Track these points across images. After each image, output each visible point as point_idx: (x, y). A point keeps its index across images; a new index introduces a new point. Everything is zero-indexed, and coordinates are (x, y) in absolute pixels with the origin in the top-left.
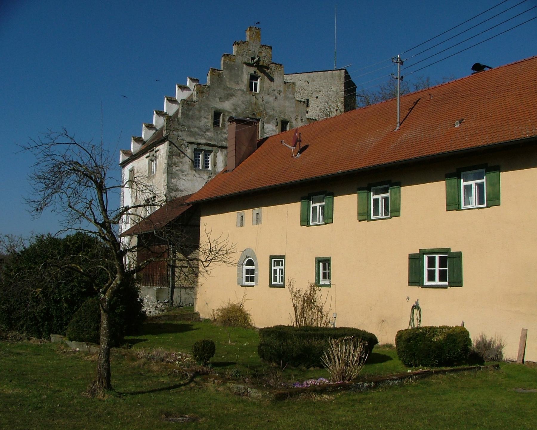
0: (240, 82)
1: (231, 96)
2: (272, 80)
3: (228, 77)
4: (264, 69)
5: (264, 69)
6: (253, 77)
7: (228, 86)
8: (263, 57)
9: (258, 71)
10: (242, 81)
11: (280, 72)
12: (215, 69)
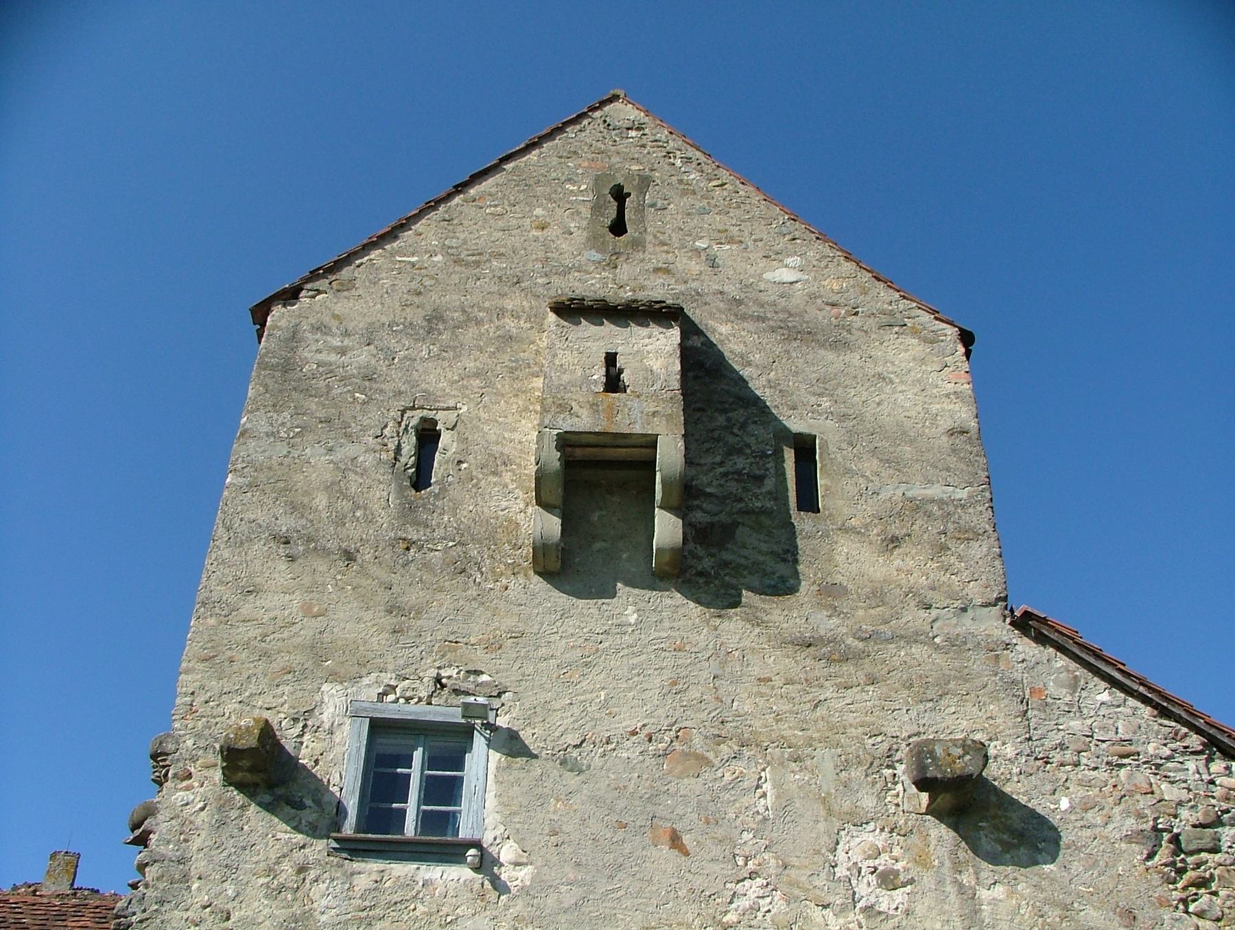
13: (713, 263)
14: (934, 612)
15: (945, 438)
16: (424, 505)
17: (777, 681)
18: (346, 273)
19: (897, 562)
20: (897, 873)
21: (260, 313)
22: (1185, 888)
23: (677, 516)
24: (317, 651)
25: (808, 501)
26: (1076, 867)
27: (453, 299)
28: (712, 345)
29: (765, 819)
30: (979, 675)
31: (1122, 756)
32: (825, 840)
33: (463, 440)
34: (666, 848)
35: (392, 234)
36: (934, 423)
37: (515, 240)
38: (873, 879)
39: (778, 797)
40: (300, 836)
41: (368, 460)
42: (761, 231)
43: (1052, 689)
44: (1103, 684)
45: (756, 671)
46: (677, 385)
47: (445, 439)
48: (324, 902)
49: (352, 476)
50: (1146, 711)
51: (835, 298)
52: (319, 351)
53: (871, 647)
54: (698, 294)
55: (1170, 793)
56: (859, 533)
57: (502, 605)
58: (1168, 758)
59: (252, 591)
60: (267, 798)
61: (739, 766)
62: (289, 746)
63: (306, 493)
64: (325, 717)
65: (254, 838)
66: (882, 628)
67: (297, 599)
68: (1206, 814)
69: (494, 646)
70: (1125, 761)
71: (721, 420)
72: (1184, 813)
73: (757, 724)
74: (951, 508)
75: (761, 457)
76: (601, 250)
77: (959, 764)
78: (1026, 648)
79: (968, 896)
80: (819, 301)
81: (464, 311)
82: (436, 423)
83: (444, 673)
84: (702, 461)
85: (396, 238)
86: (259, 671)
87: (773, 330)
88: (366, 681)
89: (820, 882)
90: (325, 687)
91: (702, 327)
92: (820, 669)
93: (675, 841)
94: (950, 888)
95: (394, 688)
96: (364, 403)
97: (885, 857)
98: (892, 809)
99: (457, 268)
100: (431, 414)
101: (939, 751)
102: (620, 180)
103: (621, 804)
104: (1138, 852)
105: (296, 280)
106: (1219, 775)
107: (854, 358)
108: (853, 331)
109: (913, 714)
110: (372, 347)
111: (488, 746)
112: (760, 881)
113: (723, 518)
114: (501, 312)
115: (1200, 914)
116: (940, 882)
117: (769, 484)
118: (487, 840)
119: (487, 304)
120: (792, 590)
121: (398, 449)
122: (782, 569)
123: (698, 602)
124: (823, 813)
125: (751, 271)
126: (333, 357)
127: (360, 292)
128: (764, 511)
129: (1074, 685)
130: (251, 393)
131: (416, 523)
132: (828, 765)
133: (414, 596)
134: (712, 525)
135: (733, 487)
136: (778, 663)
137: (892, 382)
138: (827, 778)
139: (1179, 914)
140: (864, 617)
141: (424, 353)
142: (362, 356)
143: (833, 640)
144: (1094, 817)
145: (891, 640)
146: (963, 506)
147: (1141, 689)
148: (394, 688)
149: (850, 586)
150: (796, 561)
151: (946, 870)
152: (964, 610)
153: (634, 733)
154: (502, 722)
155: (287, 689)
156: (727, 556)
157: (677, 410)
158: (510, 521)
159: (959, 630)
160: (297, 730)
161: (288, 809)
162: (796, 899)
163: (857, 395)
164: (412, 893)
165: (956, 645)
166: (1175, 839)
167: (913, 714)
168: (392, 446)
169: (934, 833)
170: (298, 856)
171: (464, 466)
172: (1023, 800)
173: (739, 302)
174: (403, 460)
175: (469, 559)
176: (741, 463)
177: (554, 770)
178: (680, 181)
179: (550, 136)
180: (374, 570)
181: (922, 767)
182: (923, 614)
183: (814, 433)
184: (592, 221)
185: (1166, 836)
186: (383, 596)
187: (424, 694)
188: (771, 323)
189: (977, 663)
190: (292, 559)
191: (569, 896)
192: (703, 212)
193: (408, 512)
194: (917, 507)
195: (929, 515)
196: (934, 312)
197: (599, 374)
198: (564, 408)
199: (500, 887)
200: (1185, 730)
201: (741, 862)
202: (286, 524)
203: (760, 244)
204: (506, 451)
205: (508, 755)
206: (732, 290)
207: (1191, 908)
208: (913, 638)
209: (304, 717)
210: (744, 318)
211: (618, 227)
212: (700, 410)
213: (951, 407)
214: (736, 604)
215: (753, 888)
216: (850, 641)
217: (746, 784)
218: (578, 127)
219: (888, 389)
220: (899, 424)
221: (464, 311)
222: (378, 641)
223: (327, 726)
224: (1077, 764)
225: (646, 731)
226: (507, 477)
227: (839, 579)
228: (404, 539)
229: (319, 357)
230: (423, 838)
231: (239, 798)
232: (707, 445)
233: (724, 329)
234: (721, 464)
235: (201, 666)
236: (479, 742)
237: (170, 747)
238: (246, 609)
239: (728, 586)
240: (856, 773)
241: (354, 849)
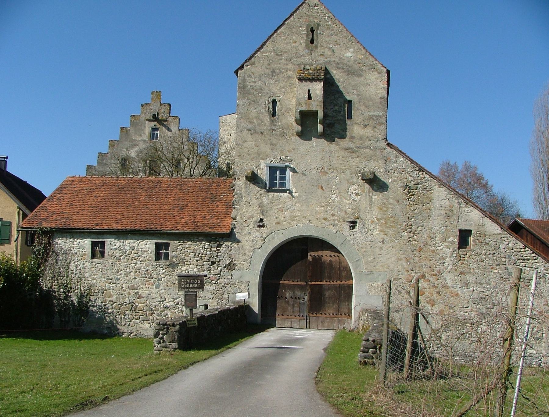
0: (142, 134)
1: (135, 146)
2: (169, 130)
3: (133, 131)
4: (163, 122)
5: (163, 122)
6: (154, 129)
7: (133, 138)
9: (158, 124)
10: (144, 133)
11: (175, 122)
12: (124, 128)
14: (372, 142)
15: (379, 100)
16: (275, 121)
17: (341, 157)
18: (253, 59)
19: (366, 131)
20: (359, 193)
21: (236, 72)
22: (409, 196)
23: (322, 125)
24: (258, 153)
25: (350, 117)
26: (390, 192)
29: (337, 184)
30: (378, 155)
31: (403, 171)
32: (347, 188)
33: (281, 105)
34: (320, 189)
35: (261, 47)
36: (378, 96)
37: (289, 47)
38: (355, 194)
39: (339, 180)
40: (260, 189)
41: (263, 110)
42: (345, 41)
43: (392, 158)
44: (402, 157)
45: (337, 155)
46: (322, 98)
47: (278, 104)
48: (265, 200)
49: (260, 115)
50: (409, 162)
51: (360, 61)
52: (250, 83)
53: (359, 149)
54: (329, 62)
56: (359, 124)
57: (291, 143)
58: (411, 172)
60: (253, 182)
61: (333, 174)
62: (256, 172)
63: (252, 119)
64: (261, 166)
65: (252, 189)
66: (361, 146)
67: (254, 143)
68: (416, 182)
69: (290, 151)
70: (403, 172)
71: (333, 97)
72: (412, 182)
73: (337, 166)
74: (378, 118)
75: (340, 106)
76: (308, 50)
77: (369, 176)
78: (388, 149)
79: (371, 197)
80: (356, 62)
81: (279, 70)
82: (276, 100)
83: (281, 157)
84: (329, 108)
85: (263, 48)
86: (249, 158)
87: (345, 72)
88: (268, 159)
89: (346, 195)
90: (261, 161)
91: (330, 72)
93: (322, 188)
94: (368, 196)
95: (273, 160)
96: (261, 96)
97: (357, 190)
98: (359, 182)
99: (277, 57)
100: (275, 98)
101: (366, 174)
102: (312, 26)
103: (313, 181)
104: (402, 189)
105: (242, 63)
106: (421, 175)
107: (362, 79)
108: (363, 71)
109: (365, 163)
110: (261, 81)
111: (290, 171)
112: (335, 195)
113: (332, 121)
114: (287, 70)
115: (411, 201)
116: (366, 195)
117: (342, 113)
118: (291, 188)
119: (284, 67)
120: (345, 138)
121: (269, 107)
122: (343, 133)
123: (327, 141)
124: (347, 183)
125: (342, 53)
126: (253, 84)
127: (257, 65)
128: (341, 120)
129: (396, 157)
130: (238, 94)
131: (274, 125)
132: (349, 173)
133: (275, 142)
134: (330, 123)
136: (341, 153)
137: (370, 85)
138: (348, 176)
139: (407, 201)
140: (358, 143)
141: (272, 82)
142: (259, 84)
143: (352, 148)
144: (395, 183)
145: (363, 148)
146: (380, 117)
147: (408, 159)
148: (273, 160)
149: (356, 137)
150: (346, 131)
151: (367, 193)
152: (378, 141)
153: (315, 168)
154: (292, 166)
155: (254, 161)
156: (333, 130)
157: (322, 104)
158: (291, 123)
159: (376, 145)
160: (257, 169)
161: (257, 184)
162: (342, 198)
163: (362, 89)
164: (279, 198)
165: (375, 149)
166: (410, 187)
167: (365, 163)
168: (268, 107)
169: (366, 186)
170: (259, 192)
171: (282, 111)
172: (383, 180)
173: (338, 64)
174: (270, 110)
175: (284, 133)
176: (336, 108)
177: (301, 175)
178: (327, 25)
179: (296, 11)
180: (267, 136)
181: (362, 177)
182: (369, 142)
183: (352, 99)
184: (306, 40)
185: (408, 186)
186: (269, 142)
187: (278, 161)
188: (345, 70)
189: (378, 153)
190: (251, 134)
191: (304, 198)
192: (332, 35)
193: (272, 123)
194: (371, 117)
195: (373, 119)
196: (382, 65)
197: (307, 96)
198: (300, 104)
199: (293, 197)
200: (416, 166)
201: (332, 191)
202: (249, 126)
203: (344, 45)
204: (290, 107)
205: (294, 173)
207: (409, 200)
208: (366, 148)
209: (258, 167)
210: (339, 68)
211: (312, 42)
212: (329, 95)
213: (382, 91)
214: (334, 141)
215: (334, 196)
216: (355, 148)
217: (334, 177)
218: (302, 7)
219: (369, 87)
220: (370, 96)
221: (279, 70)
222: (269, 151)
223: (262, 168)
224: (394, 173)
225: (317, 168)
226: (291, 113)
227: (354, 135)
228: (272, 129)
229: (250, 84)
230: (280, 189)
231: (249, 182)
232: (330, 104)
233: (335, 72)
234: (333, 108)
235: (238, 157)
236: (288, 170)
237: (236, 173)
239: (333, 137)
240: (354, 175)
241: (269, 191)
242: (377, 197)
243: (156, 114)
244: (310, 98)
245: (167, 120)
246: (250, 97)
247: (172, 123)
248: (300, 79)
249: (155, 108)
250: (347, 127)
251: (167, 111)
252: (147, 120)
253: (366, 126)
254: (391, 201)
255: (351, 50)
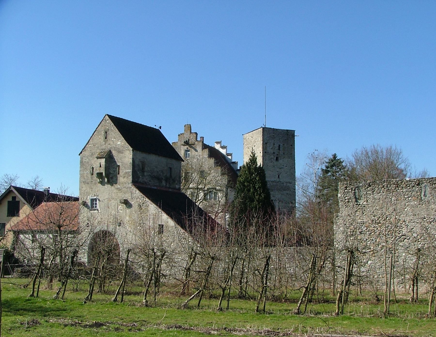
2: (196, 150)
6: (187, 151)
8: (191, 139)
9: (189, 147)
13: (113, 142)
25: (119, 174)
27: (93, 151)
28: (112, 154)
41: (89, 172)
42: (118, 136)
45: (114, 192)
51: (123, 146)
55: (140, 201)
59: (83, 188)
61: (113, 201)
92: (118, 191)
102: (106, 130)
122: (116, 181)
128: (115, 175)
133: (92, 187)
135: (113, 172)
136: (115, 191)
156: (113, 180)
190: (84, 184)
193: (92, 178)
197: (99, 166)
206: (114, 146)
211: (106, 138)
214: (113, 185)
233: (114, 152)
238: (82, 190)
242: (128, 211)
243: (188, 140)
244: (100, 166)
245: (194, 144)
246: (84, 166)
247: (198, 146)
248: (97, 158)
249: (187, 136)
250: (118, 178)
251: (194, 138)
252: (182, 145)
253: (124, 177)
254: (133, 212)
255: (120, 141)
